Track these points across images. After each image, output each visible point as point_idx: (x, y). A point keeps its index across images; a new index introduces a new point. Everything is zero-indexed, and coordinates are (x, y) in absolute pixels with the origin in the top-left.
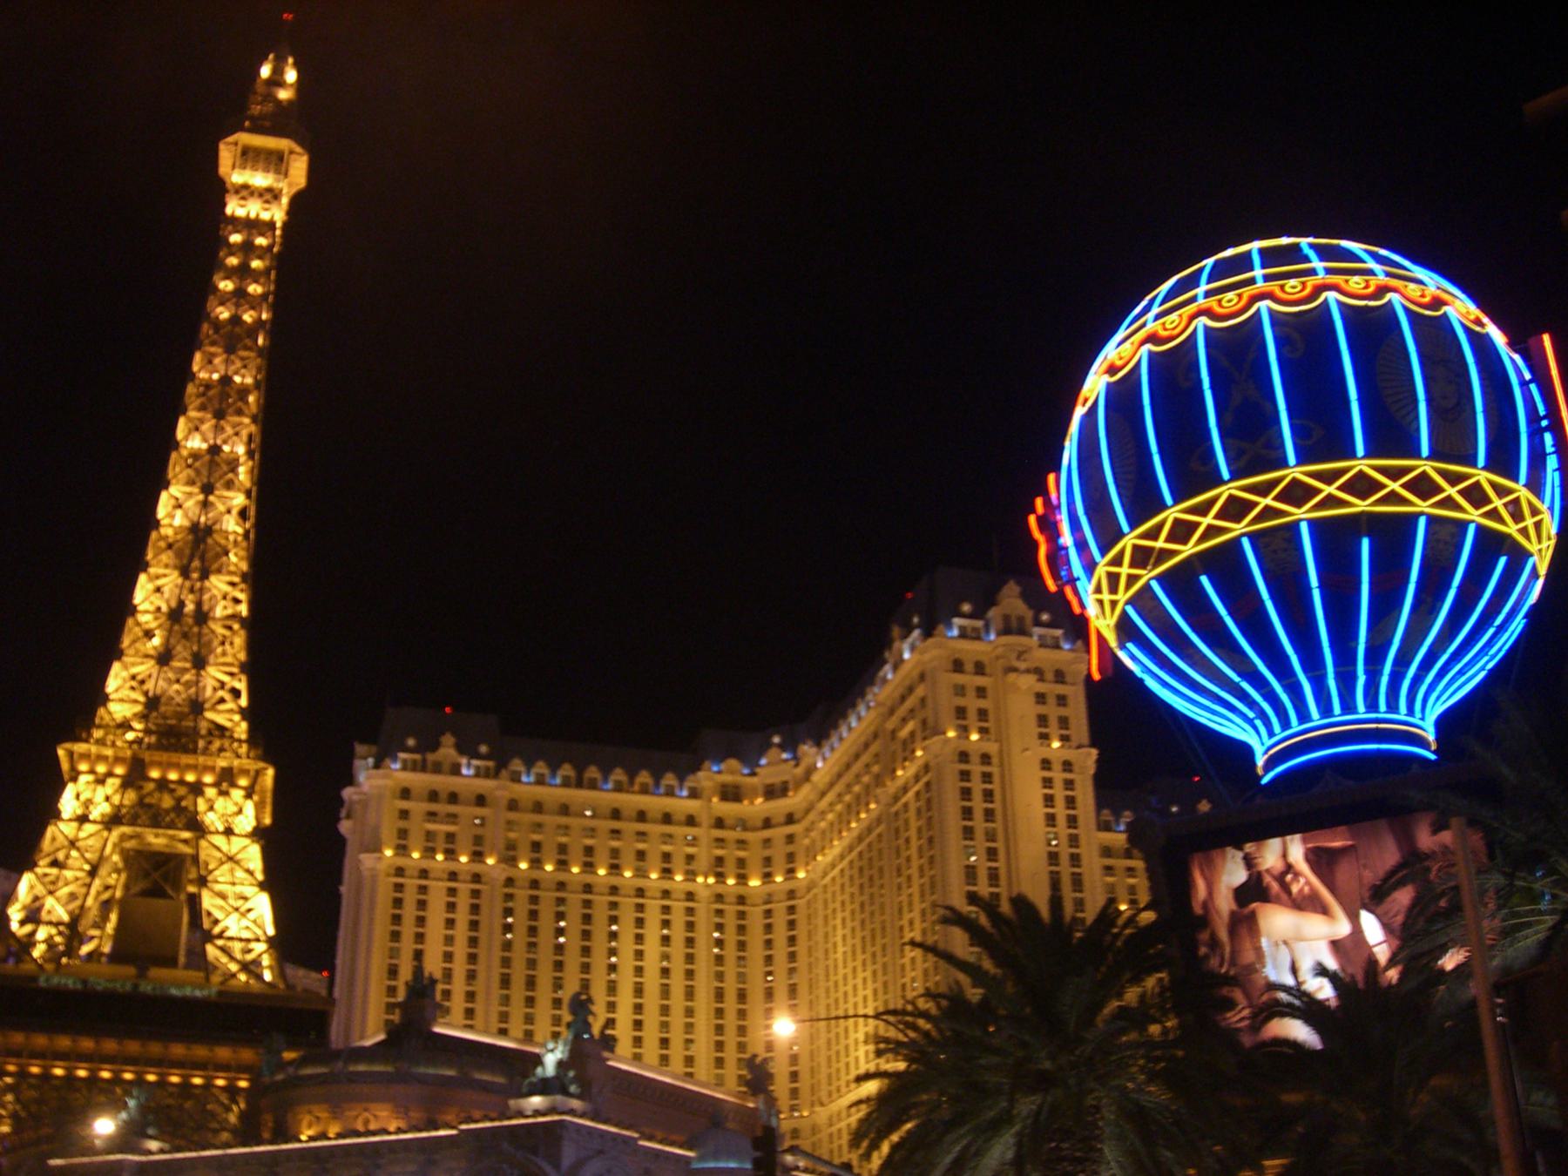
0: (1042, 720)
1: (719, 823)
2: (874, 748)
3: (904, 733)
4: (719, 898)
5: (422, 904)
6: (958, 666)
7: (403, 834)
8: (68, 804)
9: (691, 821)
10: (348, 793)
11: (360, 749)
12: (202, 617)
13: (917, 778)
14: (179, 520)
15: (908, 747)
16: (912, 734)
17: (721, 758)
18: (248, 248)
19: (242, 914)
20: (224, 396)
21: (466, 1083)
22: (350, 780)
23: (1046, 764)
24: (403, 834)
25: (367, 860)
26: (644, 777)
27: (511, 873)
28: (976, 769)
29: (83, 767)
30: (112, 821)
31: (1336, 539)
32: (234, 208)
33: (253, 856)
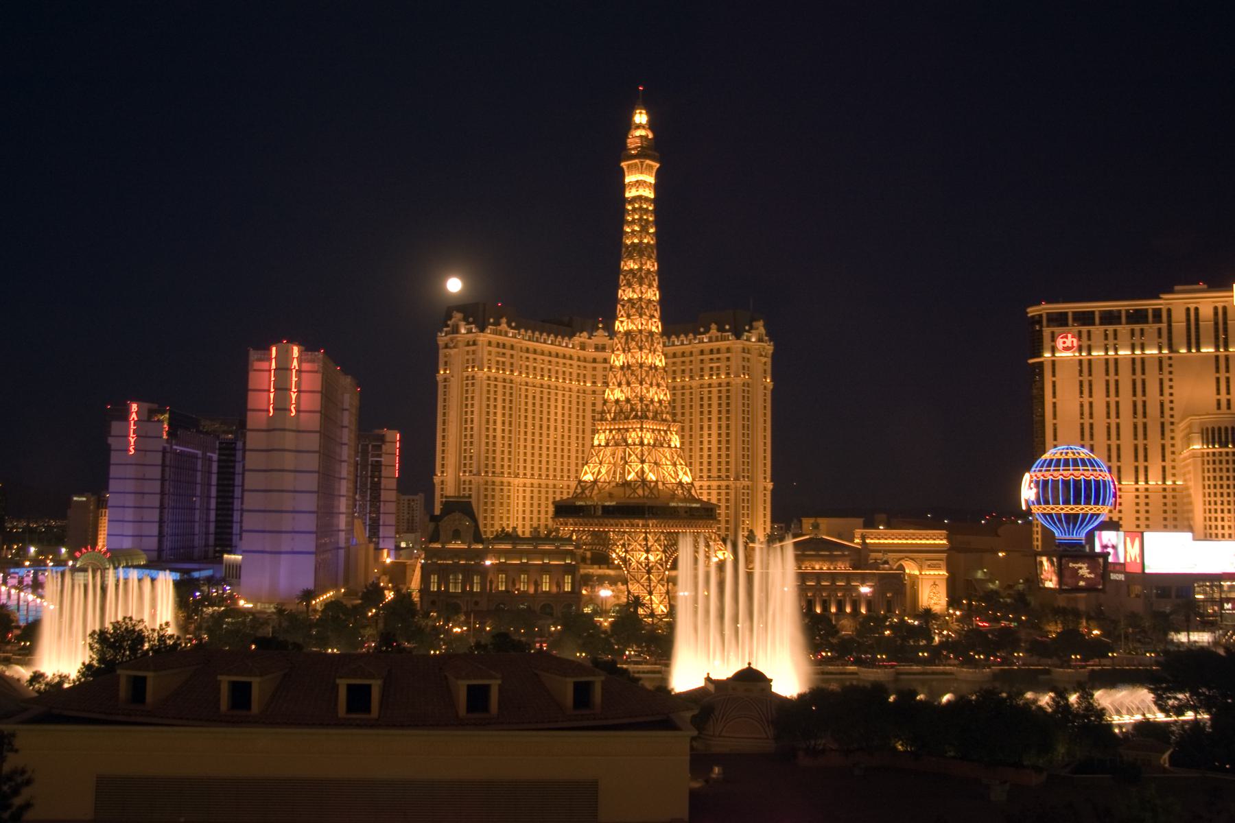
9: (571, 358)
13: (720, 385)
16: (718, 368)
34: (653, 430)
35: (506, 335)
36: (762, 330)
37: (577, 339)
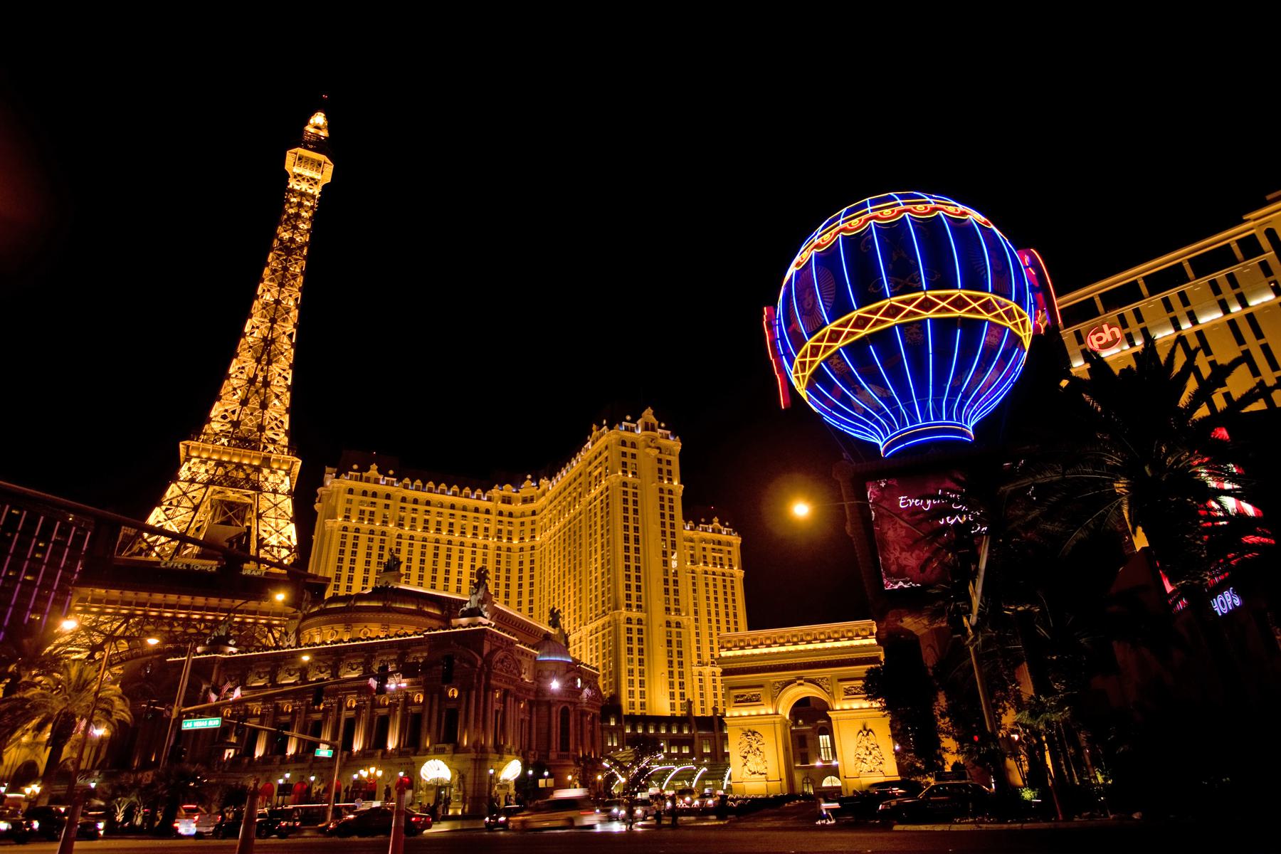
0: (660, 471)
1: (501, 514)
2: (578, 481)
3: (596, 473)
4: (499, 548)
5: (355, 545)
6: (624, 443)
7: (348, 510)
8: (184, 473)
9: (487, 512)
10: (319, 490)
11: (328, 469)
12: (266, 384)
13: (602, 493)
14: (257, 334)
15: (598, 479)
17: (501, 485)
18: (300, 205)
19: (277, 532)
20: (284, 276)
21: (419, 613)
22: (322, 484)
23: (661, 490)
24: (348, 510)
25: (329, 522)
26: (467, 490)
27: (400, 531)
28: (630, 490)
29: (194, 454)
30: (207, 484)
31: (944, 328)
32: (292, 184)
33: (287, 505)
34: (219, 463)
35: (377, 481)
36: (653, 420)
37: (496, 492)
